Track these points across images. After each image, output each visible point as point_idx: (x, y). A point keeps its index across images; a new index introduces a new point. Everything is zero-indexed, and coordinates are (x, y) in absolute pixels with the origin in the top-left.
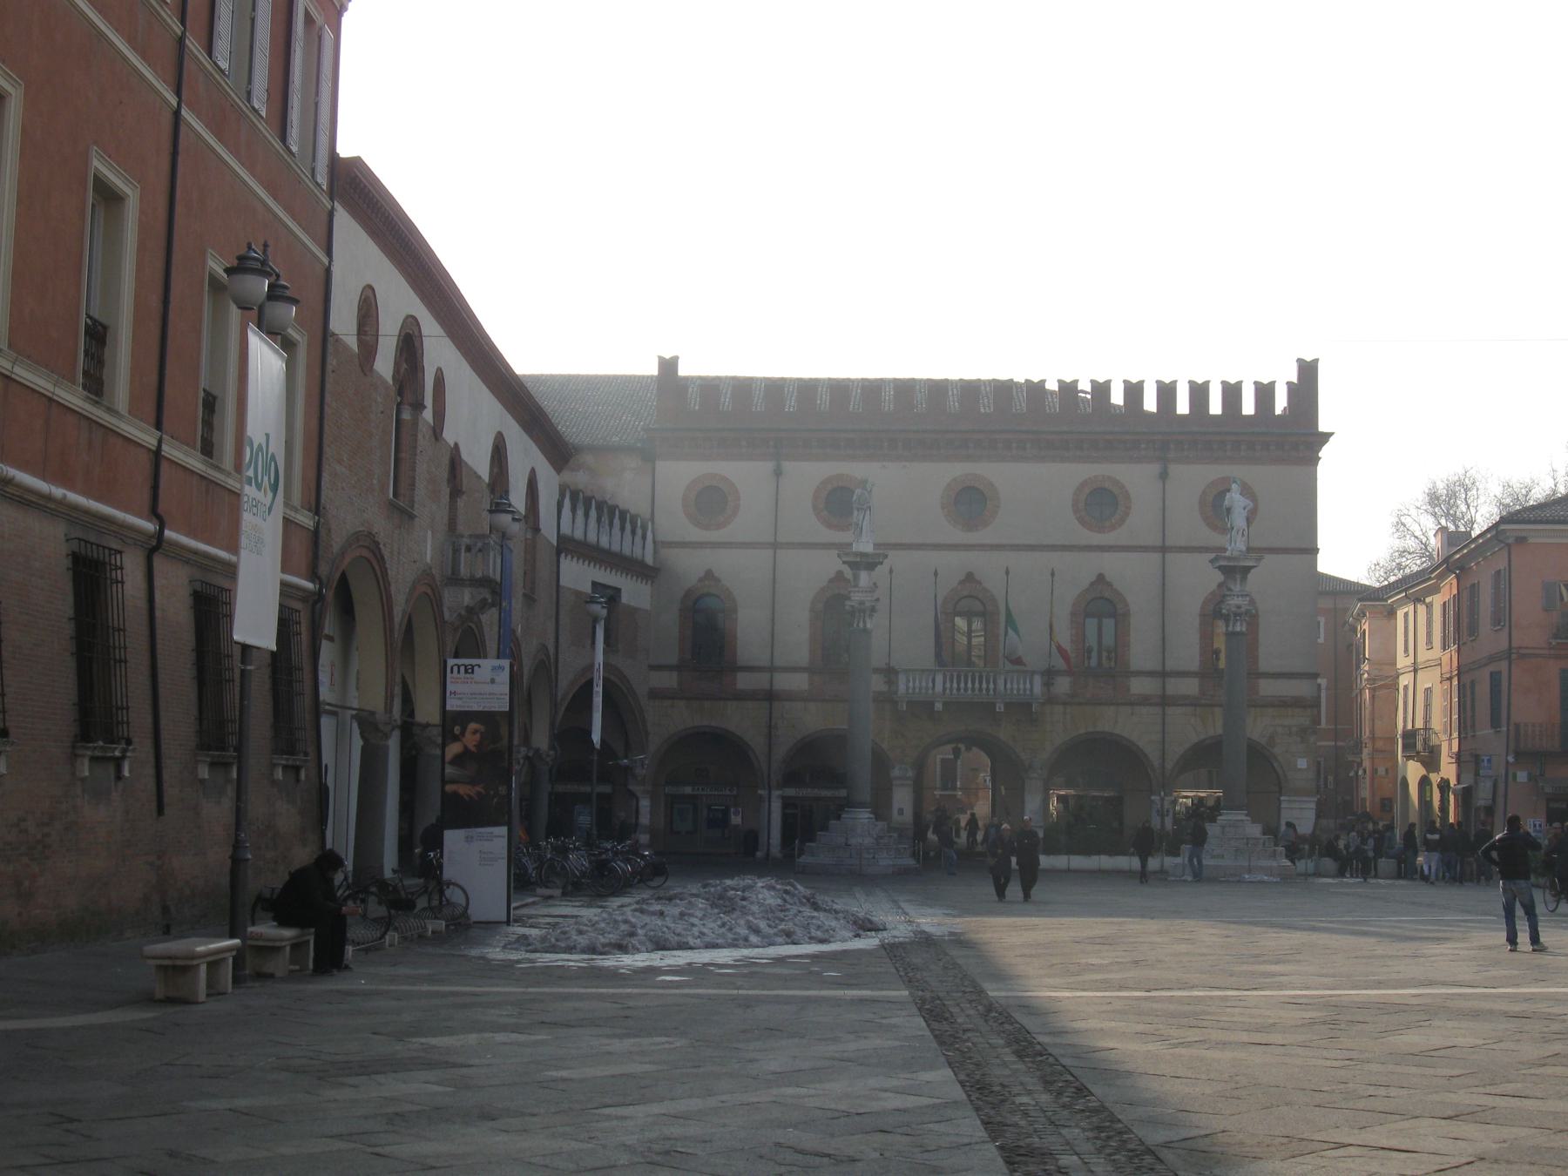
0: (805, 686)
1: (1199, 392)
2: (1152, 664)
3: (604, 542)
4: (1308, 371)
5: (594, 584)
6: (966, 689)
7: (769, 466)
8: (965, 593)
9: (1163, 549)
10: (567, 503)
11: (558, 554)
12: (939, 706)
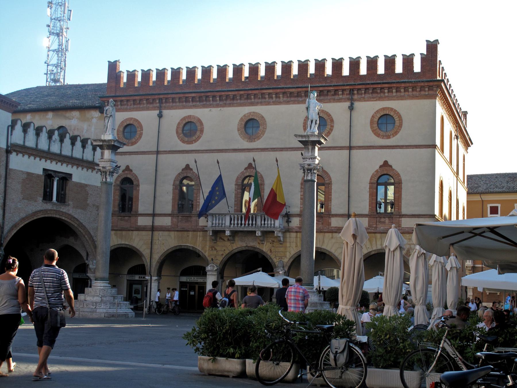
0: (170, 224)
1: (372, 62)
2: (344, 211)
3: (55, 148)
4: (432, 47)
5: (44, 170)
6: (241, 224)
7: (157, 112)
8: (248, 174)
9: (350, 148)
10: (18, 128)
11: (8, 152)
12: (228, 233)
